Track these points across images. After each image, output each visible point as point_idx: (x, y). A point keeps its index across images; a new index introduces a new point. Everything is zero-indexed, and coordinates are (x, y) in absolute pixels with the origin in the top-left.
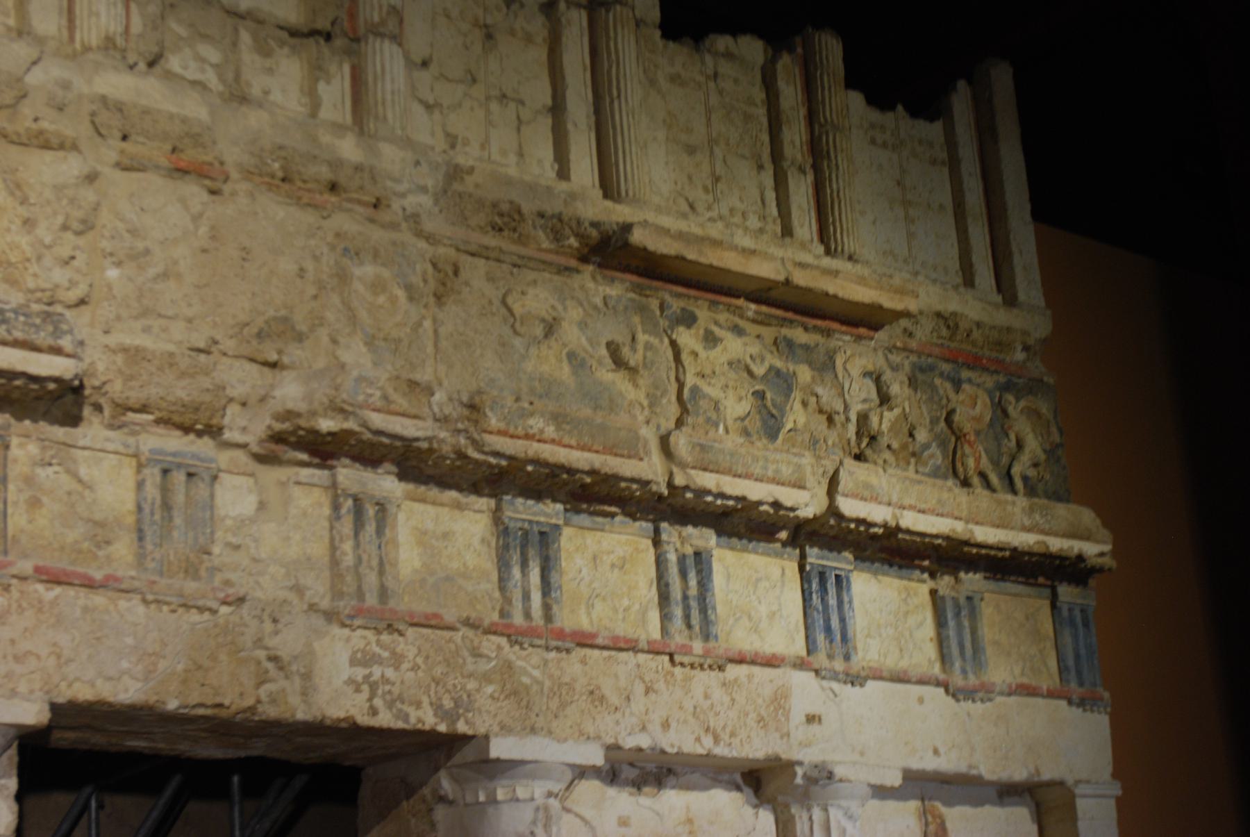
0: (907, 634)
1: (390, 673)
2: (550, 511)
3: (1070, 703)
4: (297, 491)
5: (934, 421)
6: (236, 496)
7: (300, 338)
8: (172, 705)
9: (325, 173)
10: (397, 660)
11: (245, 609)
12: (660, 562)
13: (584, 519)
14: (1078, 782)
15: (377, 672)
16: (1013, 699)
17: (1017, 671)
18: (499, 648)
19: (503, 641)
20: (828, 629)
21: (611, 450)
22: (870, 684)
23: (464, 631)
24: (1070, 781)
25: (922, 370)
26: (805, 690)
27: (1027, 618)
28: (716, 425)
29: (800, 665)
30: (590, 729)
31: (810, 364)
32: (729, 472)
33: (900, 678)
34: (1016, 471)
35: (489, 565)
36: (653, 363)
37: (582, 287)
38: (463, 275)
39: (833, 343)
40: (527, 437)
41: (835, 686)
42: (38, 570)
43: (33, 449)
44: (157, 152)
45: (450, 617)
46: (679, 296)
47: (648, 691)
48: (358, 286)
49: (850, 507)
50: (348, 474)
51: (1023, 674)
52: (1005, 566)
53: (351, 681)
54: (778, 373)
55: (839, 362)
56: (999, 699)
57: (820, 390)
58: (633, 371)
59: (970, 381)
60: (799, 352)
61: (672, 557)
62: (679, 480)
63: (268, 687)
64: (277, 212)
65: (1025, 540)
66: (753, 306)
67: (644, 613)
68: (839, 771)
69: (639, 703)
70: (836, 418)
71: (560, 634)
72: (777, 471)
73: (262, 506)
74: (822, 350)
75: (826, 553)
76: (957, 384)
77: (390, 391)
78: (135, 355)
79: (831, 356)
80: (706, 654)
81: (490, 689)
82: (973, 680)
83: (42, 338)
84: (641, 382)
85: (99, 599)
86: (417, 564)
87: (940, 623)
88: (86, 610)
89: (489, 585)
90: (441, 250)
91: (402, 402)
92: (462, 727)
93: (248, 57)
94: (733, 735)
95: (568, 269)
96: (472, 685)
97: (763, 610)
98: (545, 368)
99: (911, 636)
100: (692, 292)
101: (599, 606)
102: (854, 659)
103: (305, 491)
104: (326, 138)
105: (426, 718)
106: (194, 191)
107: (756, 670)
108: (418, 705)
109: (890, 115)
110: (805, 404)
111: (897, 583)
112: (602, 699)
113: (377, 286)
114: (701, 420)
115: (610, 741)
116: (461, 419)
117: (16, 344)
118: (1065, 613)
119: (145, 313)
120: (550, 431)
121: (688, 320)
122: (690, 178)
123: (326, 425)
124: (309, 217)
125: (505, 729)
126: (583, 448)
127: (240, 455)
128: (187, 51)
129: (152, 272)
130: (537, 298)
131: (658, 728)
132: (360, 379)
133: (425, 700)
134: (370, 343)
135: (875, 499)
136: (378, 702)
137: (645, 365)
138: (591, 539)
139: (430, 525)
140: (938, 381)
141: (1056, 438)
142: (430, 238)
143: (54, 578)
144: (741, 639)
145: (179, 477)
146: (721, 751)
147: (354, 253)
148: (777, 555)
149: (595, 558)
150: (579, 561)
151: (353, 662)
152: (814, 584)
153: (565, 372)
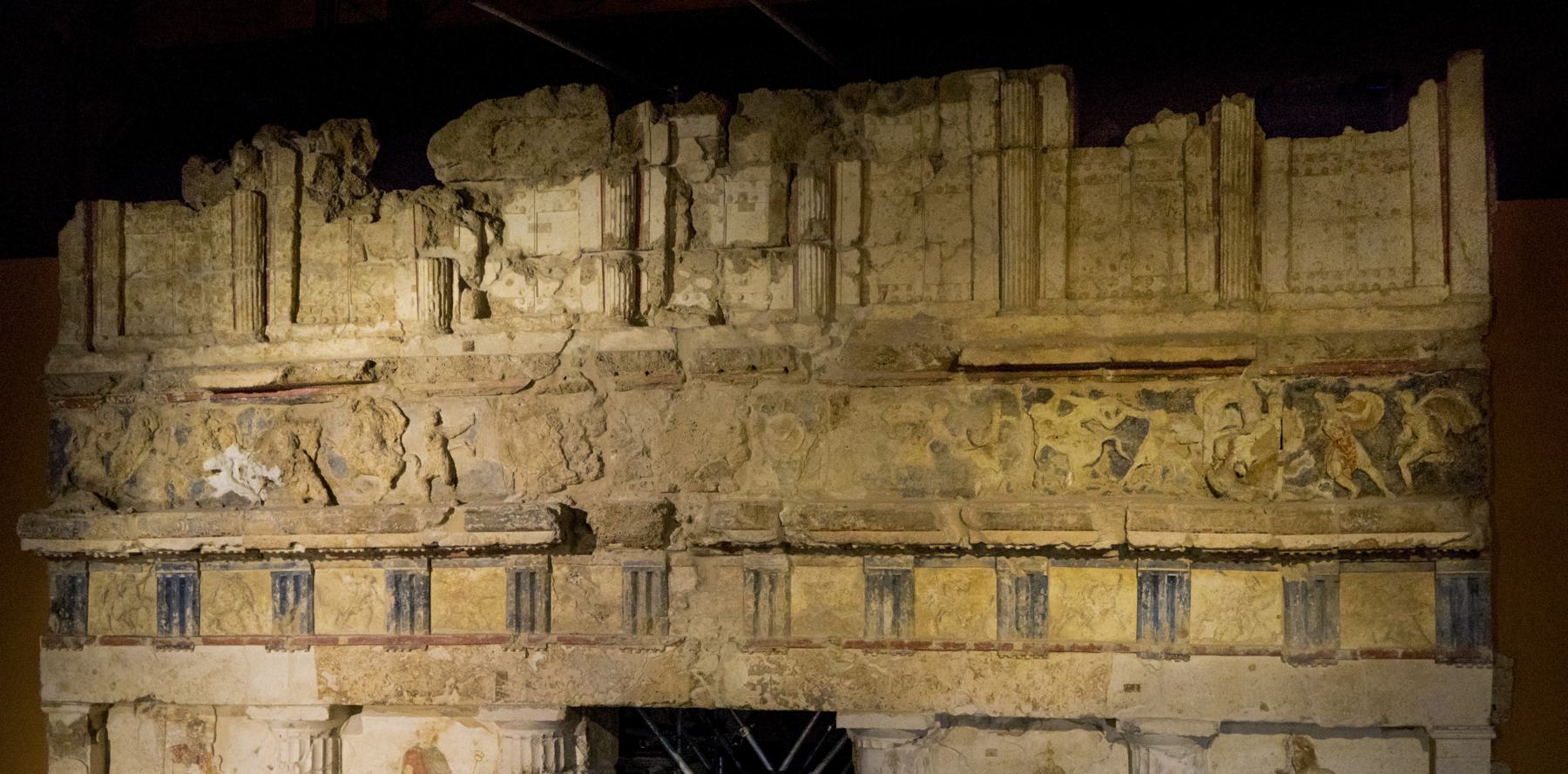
0: (1250, 615)
1: (776, 678)
2: (904, 561)
3: (1437, 662)
4: (723, 572)
5: (1310, 431)
6: (682, 580)
7: (731, 474)
8: (639, 704)
9: (745, 360)
10: (781, 669)
11: (686, 648)
12: (999, 585)
13: (936, 562)
14: (1437, 728)
15: (767, 678)
16: (1361, 662)
17: (1379, 636)
18: (856, 656)
19: (859, 652)
20: (1156, 620)
21: (912, 528)
22: (1195, 659)
23: (831, 647)
24: (1429, 727)
25: (1299, 389)
26: (1125, 667)
27: (1401, 589)
28: (1065, 474)
29: (1122, 648)
30: (926, 705)
31: (1168, 410)
32: (1017, 528)
33: (1230, 652)
34: (1403, 462)
35: (859, 599)
36: (1008, 436)
37: (954, 391)
38: (853, 403)
39: (1197, 383)
40: (844, 529)
41: (1154, 662)
42: (560, 639)
43: (565, 569)
44: (639, 377)
45: (818, 638)
46: (1039, 379)
47: (976, 676)
48: (769, 431)
49: (1138, 539)
50: (750, 559)
51: (1387, 638)
52: (1346, 555)
53: (749, 684)
54: (1134, 420)
55: (1199, 401)
56: (1342, 663)
57: (1176, 427)
58: (987, 449)
59: (1361, 388)
60: (1159, 399)
61: (1007, 581)
62: (975, 540)
63: (698, 690)
64: (717, 391)
65: (1353, 540)
66: (1111, 372)
67: (984, 618)
68: (1145, 727)
69: (969, 683)
70: (1192, 447)
71: (899, 645)
72: (1062, 522)
73: (699, 585)
74: (1183, 394)
75: (1159, 561)
76: (1342, 393)
77: (741, 516)
78: (614, 509)
79: (1191, 396)
80: (1026, 647)
81: (848, 683)
82: (1313, 649)
83: (530, 524)
84: (995, 454)
85: (596, 650)
86: (804, 606)
87: (1287, 605)
88: (589, 656)
89: (858, 615)
90: (837, 390)
91: (750, 522)
92: (826, 707)
93: (730, 277)
94: (1051, 702)
95: (941, 380)
96: (834, 681)
97: (1097, 609)
98: (909, 460)
99: (1255, 615)
100: (1051, 374)
101: (945, 619)
102: (1179, 641)
103: (727, 571)
104: (753, 333)
105: (802, 704)
106: (661, 394)
107: (1079, 656)
108: (796, 696)
109: (1336, 140)
110: (1161, 440)
111: (1244, 574)
112: (937, 684)
113: (784, 427)
114: (1051, 471)
115: (940, 711)
116: (799, 523)
117: (518, 530)
118: (1446, 583)
119: (632, 477)
120: (861, 523)
121: (1044, 396)
122: (1098, 262)
123: (707, 541)
124: (739, 391)
125: (858, 709)
126: (889, 530)
127: (684, 556)
128: (690, 287)
129: (634, 452)
130: (912, 406)
131: (984, 701)
132: (720, 513)
133: (800, 692)
134: (777, 467)
135: (1166, 528)
136: (767, 695)
137: (1000, 440)
138: (942, 576)
139: (815, 580)
140: (1317, 395)
141: (1476, 419)
142: (829, 383)
143: (569, 642)
144: (1074, 632)
145: (642, 576)
146: (1035, 714)
147: (769, 409)
148: (1113, 566)
149: (944, 586)
150: (931, 590)
151: (751, 672)
152: (1149, 583)
153: (928, 459)
